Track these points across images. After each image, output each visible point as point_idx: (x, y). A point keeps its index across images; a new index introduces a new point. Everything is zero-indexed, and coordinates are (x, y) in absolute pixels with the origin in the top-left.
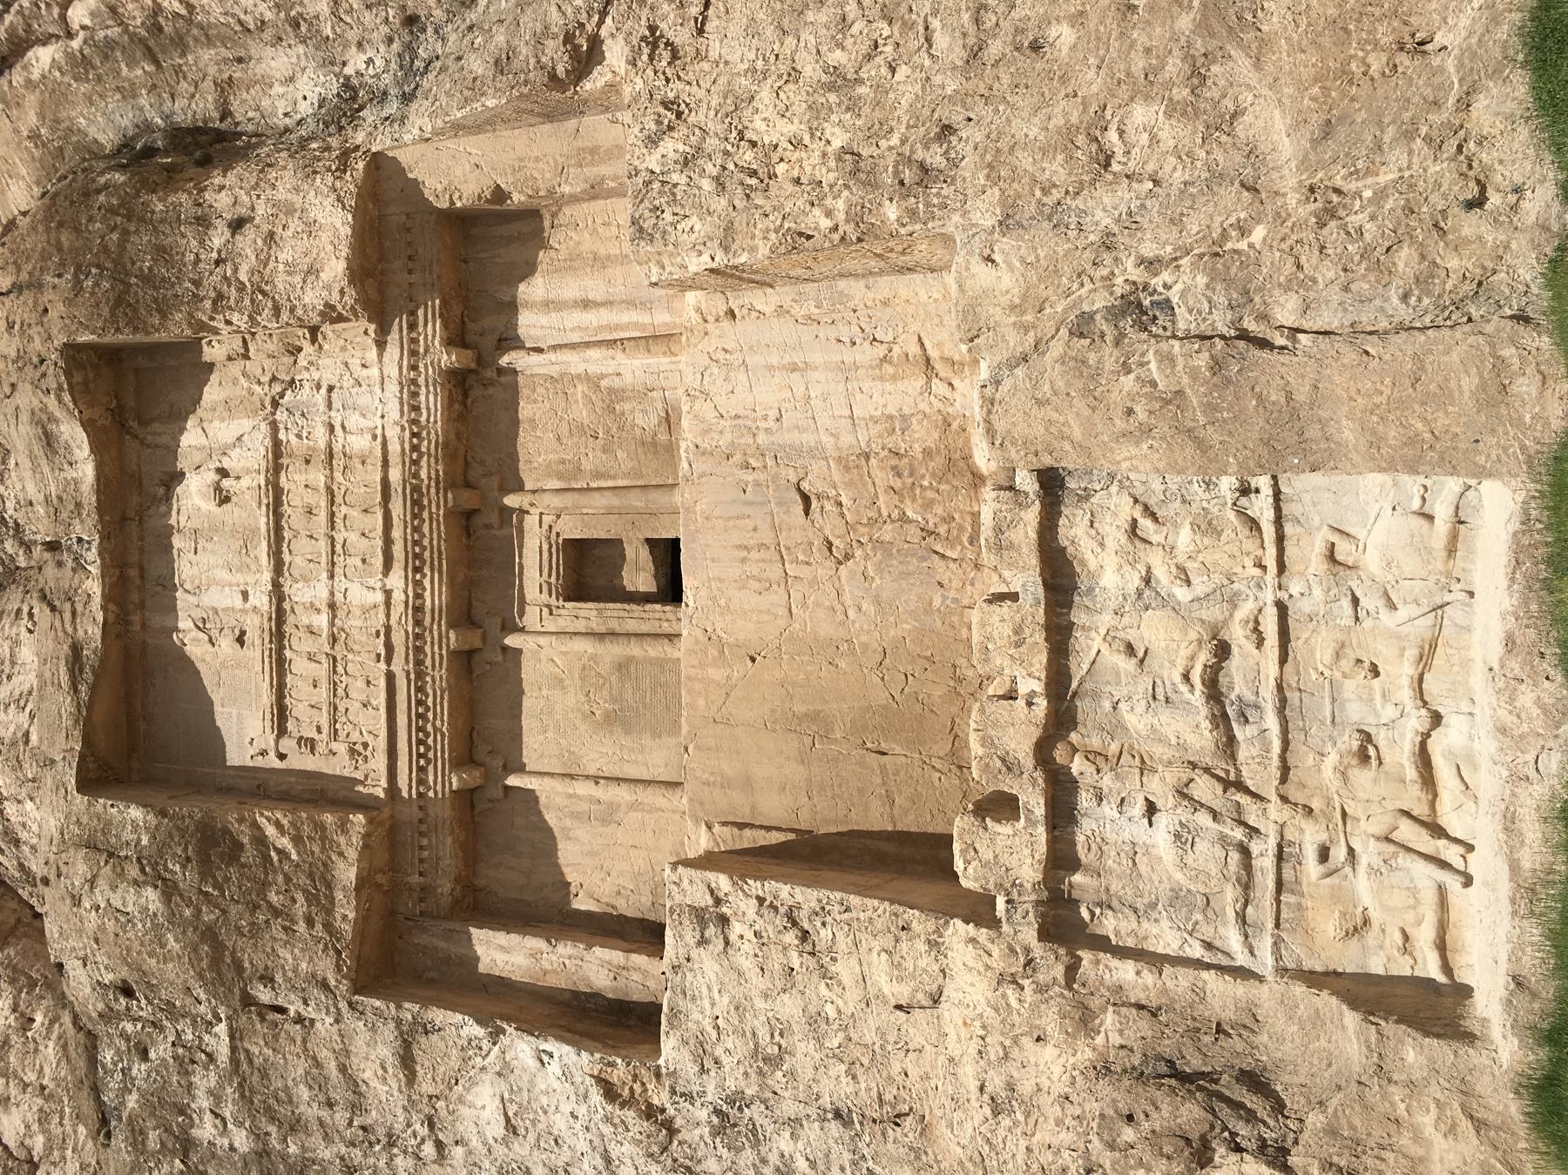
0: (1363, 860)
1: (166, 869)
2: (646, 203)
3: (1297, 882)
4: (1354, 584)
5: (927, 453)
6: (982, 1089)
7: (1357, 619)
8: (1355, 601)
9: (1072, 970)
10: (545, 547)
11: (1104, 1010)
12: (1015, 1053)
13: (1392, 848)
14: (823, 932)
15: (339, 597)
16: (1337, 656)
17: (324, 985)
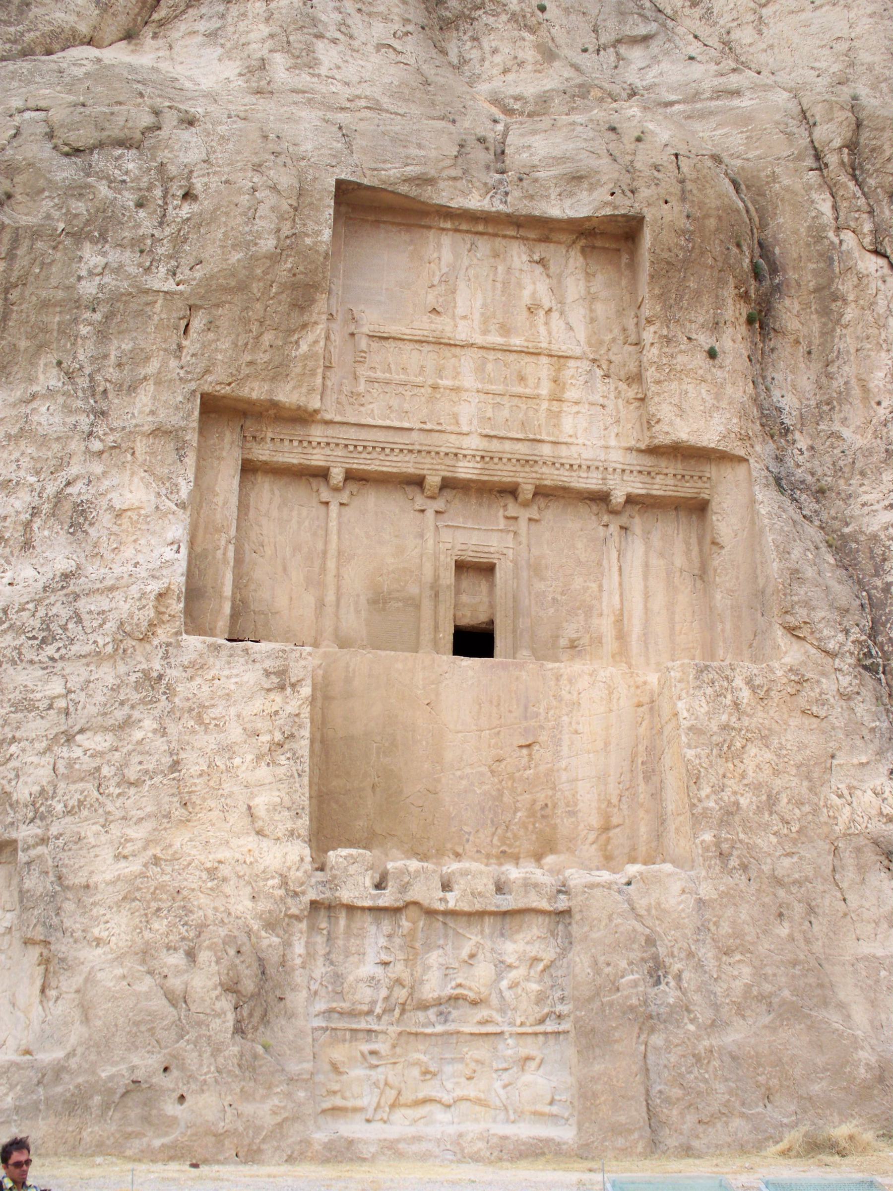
0: (372, 1073)
1: (288, 256)
2: (717, 676)
3: (356, 1040)
4: (515, 1069)
5: (554, 827)
6: (220, 862)
7: (497, 1070)
8: (506, 1069)
9: (298, 918)
10: (492, 550)
11: (278, 936)
12: (242, 883)
13: (382, 1086)
14: (283, 758)
15: (464, 396)
16: (477, 1061)
17: (207, 371)
